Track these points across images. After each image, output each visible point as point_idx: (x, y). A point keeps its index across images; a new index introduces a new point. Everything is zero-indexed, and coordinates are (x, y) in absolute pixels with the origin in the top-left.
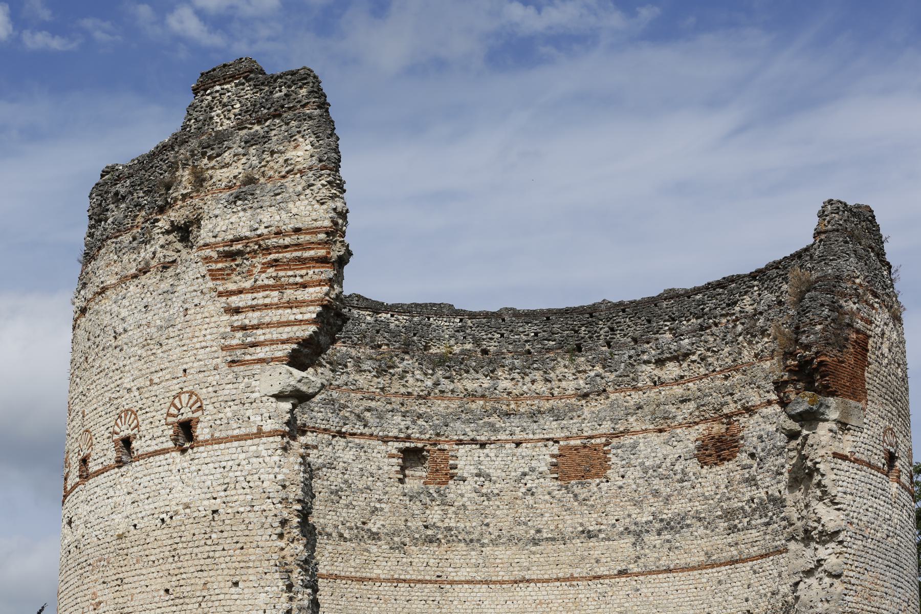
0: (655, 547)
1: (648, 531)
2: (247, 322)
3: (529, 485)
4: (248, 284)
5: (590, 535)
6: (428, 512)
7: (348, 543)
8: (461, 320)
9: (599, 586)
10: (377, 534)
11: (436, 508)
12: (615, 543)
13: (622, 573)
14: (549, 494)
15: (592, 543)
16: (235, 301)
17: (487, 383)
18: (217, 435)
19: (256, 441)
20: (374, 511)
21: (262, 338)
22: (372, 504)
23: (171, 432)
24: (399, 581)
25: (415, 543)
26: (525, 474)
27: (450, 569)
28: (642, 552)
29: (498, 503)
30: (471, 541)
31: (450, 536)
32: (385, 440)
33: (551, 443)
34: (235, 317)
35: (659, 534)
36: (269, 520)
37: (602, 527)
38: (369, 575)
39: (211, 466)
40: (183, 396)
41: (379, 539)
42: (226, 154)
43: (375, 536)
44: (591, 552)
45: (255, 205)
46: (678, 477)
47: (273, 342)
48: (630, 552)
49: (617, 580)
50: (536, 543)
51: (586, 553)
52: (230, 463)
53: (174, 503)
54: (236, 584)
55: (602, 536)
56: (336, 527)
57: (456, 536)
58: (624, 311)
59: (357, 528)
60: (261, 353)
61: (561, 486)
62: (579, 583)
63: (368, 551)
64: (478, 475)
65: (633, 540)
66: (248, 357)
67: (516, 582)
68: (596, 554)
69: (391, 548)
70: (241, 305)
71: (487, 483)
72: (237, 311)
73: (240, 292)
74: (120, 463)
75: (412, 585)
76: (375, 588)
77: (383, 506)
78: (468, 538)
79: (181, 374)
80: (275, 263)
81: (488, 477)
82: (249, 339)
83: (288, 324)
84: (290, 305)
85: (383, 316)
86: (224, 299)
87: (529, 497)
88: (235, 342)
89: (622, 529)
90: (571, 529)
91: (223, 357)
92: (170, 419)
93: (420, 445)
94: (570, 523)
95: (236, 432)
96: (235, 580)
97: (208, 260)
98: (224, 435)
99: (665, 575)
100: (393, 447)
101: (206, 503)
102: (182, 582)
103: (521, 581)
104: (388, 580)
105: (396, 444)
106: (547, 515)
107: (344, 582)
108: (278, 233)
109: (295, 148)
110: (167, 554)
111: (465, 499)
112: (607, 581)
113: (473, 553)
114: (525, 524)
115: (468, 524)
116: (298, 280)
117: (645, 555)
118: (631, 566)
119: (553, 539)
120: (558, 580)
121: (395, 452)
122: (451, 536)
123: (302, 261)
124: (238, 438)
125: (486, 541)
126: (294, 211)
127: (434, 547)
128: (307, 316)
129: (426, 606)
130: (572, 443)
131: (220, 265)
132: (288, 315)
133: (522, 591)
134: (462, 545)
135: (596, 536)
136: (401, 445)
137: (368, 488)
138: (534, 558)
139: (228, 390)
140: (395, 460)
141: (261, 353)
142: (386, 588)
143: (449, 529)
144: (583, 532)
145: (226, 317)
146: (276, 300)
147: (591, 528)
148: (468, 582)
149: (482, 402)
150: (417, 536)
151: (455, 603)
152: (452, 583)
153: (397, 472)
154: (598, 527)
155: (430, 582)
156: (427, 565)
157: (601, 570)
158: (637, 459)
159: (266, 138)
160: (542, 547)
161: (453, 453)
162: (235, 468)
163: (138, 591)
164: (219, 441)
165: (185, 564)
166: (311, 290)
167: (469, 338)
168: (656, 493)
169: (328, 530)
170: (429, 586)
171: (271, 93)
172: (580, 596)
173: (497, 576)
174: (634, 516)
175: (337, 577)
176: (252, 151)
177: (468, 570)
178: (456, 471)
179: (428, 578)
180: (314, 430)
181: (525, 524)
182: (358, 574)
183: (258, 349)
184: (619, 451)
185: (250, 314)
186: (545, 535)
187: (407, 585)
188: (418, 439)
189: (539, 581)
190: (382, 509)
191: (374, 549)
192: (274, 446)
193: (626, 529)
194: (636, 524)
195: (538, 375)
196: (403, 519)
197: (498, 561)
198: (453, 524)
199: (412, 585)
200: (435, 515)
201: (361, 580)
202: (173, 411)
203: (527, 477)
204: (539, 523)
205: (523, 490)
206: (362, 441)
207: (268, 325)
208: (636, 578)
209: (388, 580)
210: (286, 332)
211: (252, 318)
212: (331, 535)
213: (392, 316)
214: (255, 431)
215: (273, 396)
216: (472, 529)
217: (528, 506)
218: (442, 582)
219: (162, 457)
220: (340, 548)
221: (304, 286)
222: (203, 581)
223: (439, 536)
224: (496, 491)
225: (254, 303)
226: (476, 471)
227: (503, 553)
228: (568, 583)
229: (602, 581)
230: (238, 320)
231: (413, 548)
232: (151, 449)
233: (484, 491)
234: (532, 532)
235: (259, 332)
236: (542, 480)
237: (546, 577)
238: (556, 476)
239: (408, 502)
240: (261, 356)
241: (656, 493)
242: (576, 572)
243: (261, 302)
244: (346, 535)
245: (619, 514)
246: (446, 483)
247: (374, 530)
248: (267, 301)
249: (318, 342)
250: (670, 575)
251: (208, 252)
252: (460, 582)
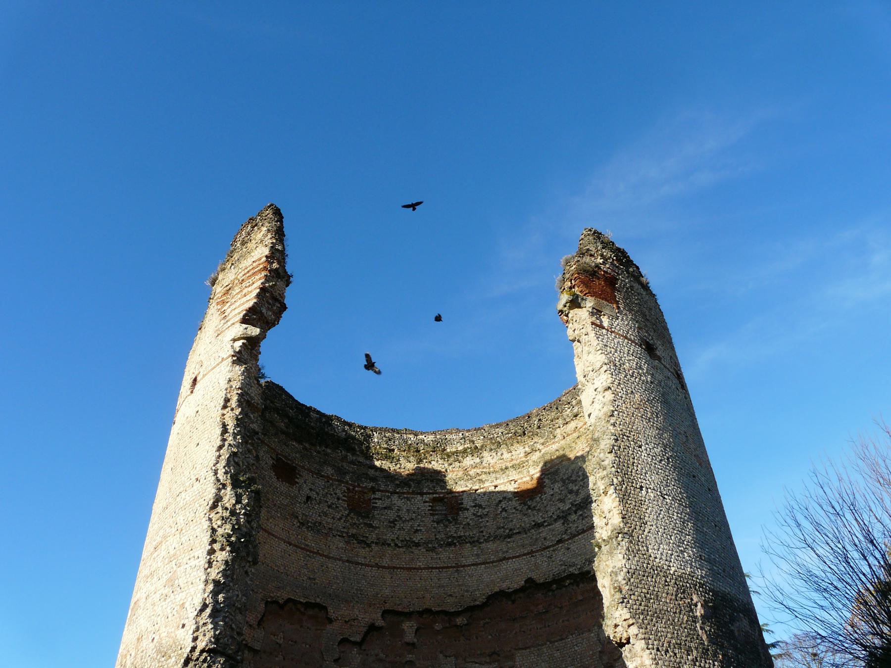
0: (574, 521)
1: (570, 514)
3: (503, 507)
5: (538, 525)
6: (448, 530)
7: (401, 549)
8: (463, 435)
9: (548, 553)
10: (418, 543)
11: (453, 527)
12: (553, 526)
13: (560, 541)
14: (515, 508)
15: (542, 529)
17: (478, 460)
20: (417, 531)
22: (415, 528)
24: (432, 568)
25: (441, 546)
26: (500, 501)
27: (462, 559)
28: (569, 526)
29: (487, 519)
30: (474, 542)
31: (462, 540)
32: (422, 494)
33: (513, 482)
35: (576, 513)
37: (546, 519)
38: (414, 566)
41: (420, 546)
43: (417, 545)
44: (541, 535)
46: (581, 478)
47: (236, 315)
48: (562, 529)
49: (557, 546)
50: (509, 536)
51: (538, 536)
55: (546, 524)
56: (392, 540)
57: (465, 540)
58: (544, 409)
59: (406, 540)
61: (521, 503)
62: (537, 554)
63: (412, 552)
64: (474, 506)
65: (562, 521)
67: (501, 560)
68: (544, 534)
69: (427, 550)
71: (480, 510)
75: (441, 570)
76: (418, 574)
77: (421, 528)
78: (471, 540)
81: (480, 506)
83: (243, 304)
84: (245, 296)
85: (420, 437)
87: (504, 513)
89: (556, 517)
90: (529, 525)
93: (441, 495)
94: (527, 521)
99: (582, 535)
100: (426, 498)
103: (504, 560)
104: (424, 569)
105: (428, 496)
106: (515, 520)
107: (399, 570)
111: (468, 520)
112: (552, 549)
113: (475, 548)
114: (503, 527)
115: (471, 534)
117: (570, 528)
118: (564, 536)
119: (519, 533)
120: (524, 555)
121: (427, 500)
122: (462, 540)
125: (482, 541)
127: (453, 548)
129: (450, 582)
130: (525, 479)
132: (245, 299)
133: (505, 565)
134: (468, 545)
135: (543, 525)
136: (431, 496)
137: (412, 519)
138: (509, 545)
140: (427, 504)
142: (425, 573)
143: (460, 537)
144: (535, 525)
147: (539, 522)
148: (473, 565)
149: (475, 470)
150: (442, 543)
151: (466, 578)
152: (464, 566)
153: (429, 510)
154: (543, 520)
155: (451, 567)
156: (449, 558)
157: (548, 543)
158: (559, 477)
160: (514, 538)
161: (460, 497)
167: (468, 442)
168: (571, 492)
169: (388, 542)
170: (451, 569)
172: (538, 561)
173: (490, 559)
174: (561, 508)
175: (394, 568)
177: (473, 558)
178: (463, 506)
179: (449, 565)
180: (379, 490)
181: (503, 527)
182: (408, 566)
184: (549, 476)
186: (515, 532)
187: (437, 570)
188: (442, 493)
189: (514, 557)
190: (421, 530)
191: (416, 552)
192: (227, 363)
193: (558, 516)
194: (563, 512)
195: (504, 451)
196: (433, 534)
197: (490, 550)
198: (462, 534)
199: (441, 570)
200: (452, 529)
201: (409, 569)
203: (502, 503)
204: (510, 525)
205: (500, 510)
206: (409, 496)
208: (567, 542)
209: (424, 569)
212: (390, 544)
213: (425, 436)
216: (473, 536)
217: (504, 518)
218: (458, 567)
220: (395, 552)
223: (455, 541)
224: (486, 513)
226: (473, 505)
227: (491, 546)
228: (530, 556)
229: (548, 549)
231: (441, 550)
233: (479, 514)
234: (508, 531)
236: (510, 502)
237: (517, 554)
238: (517, 498)
239: (436, 525)
241: (571, 492)
242: (534, 548)
244: (400, 545)
245: (553, 509)
246: (458, 514)
247: (417, 541)
249: (261, 311)
250: (585, 534)
252: (469, 565)
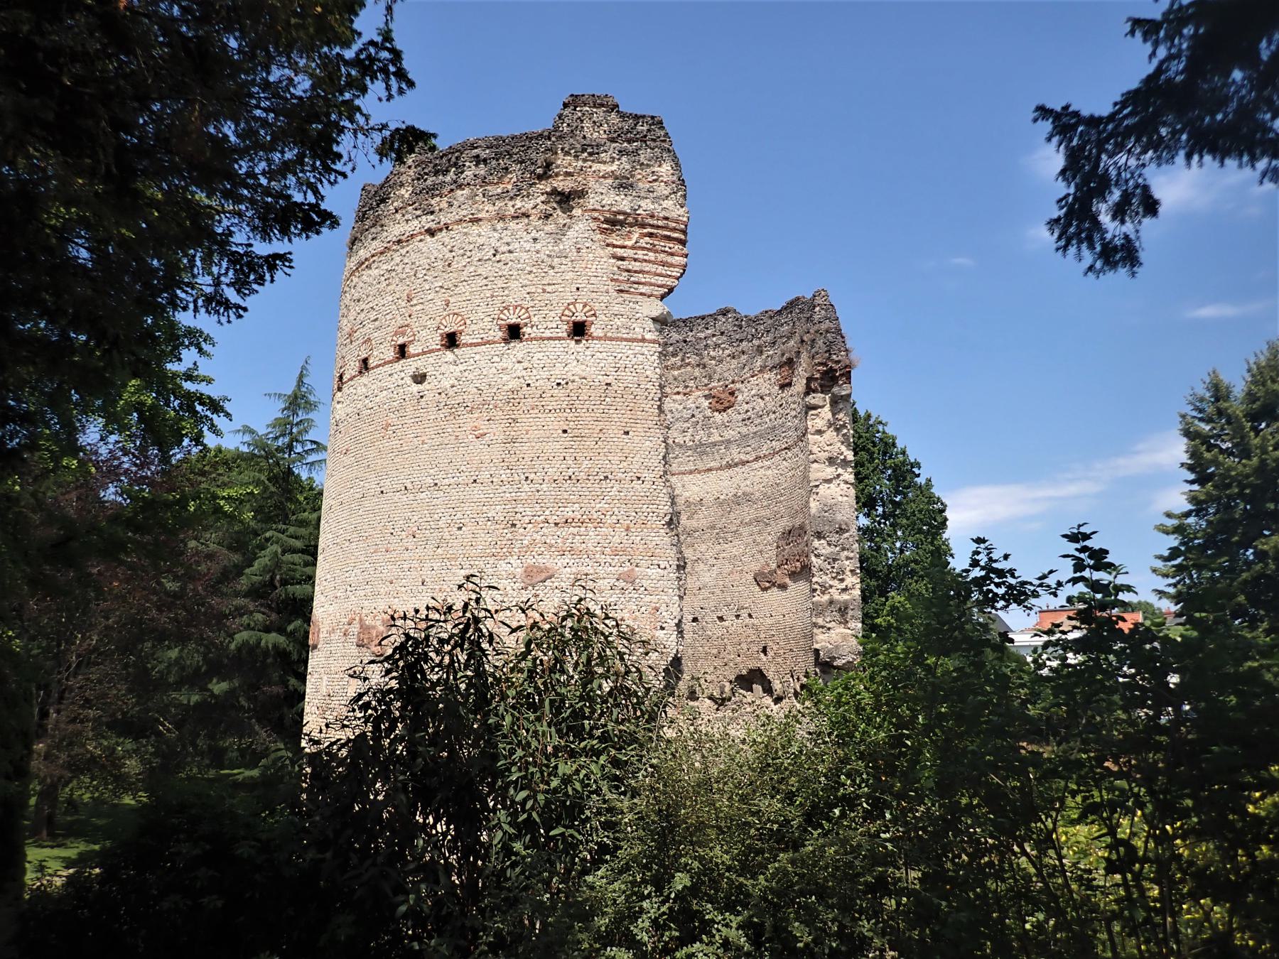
2: (630, 267)
4: (629, 243)
16: (620, 252)
18: (609, 334)
19: (641, 344)
21: (643, 280)
23: (566, 327)
34: (620, 262)
36: (652, 395)
39: (604, 354)
40: (577, 305)
42: (602, 155)
45: (634, 194)
47: (651, 284)
52: (620, 355)
53: (570, 374)
54: (627, 433)
60: (643, 289)
66: (632, 290)
70: (625, 255)
72: (622, 259)
73: (624, 247)
74: (506, 341)
79: (575, 290)
80: (651, 235)
82: (632, 279)
84: (664, 264)
86: (609, 248)
88: (621, 278)
91: (612, 287)
92: (563, 318)
95: (625, 336)
96: (627, 429)
97: (595, 219)
98: (615, 335)
101: (600, 377)
102: (579, 427)
108: (652, 216)
109: (660, 166)
110: (564, 406)
116: (667, 249)
123: (668, 238)
124: (626, 340)
126: (665, 206)
128: (674, 274)
131: (605, 226)
132: (660, 269)
139: (616, 309)
141: (643, 289)
145: (614, 261)
146: (653, 259)
159: (636, 152)
162: (624, 358)
163: (535, 428)
164: (611, 339)
165: (582, 415)
166: (677, 258)
171: (636, 125)
176: (624, 159)
183: (641, 286)
185: (633, 263)
202: (567, 312)
207: (648, 272)
210: (660, 280)
211: (636, 266)
214: (640, 337)
215: (652, 319)
219: (557, 342)
221: (672, 254)
222: (599, 428)
225: (636, 256)
230: (625, 264)
232: (544, 335)
235: (641, 275)
240: (643, 291)
243: (641, 257)
248: (646, 257)
251: (596, 215)
